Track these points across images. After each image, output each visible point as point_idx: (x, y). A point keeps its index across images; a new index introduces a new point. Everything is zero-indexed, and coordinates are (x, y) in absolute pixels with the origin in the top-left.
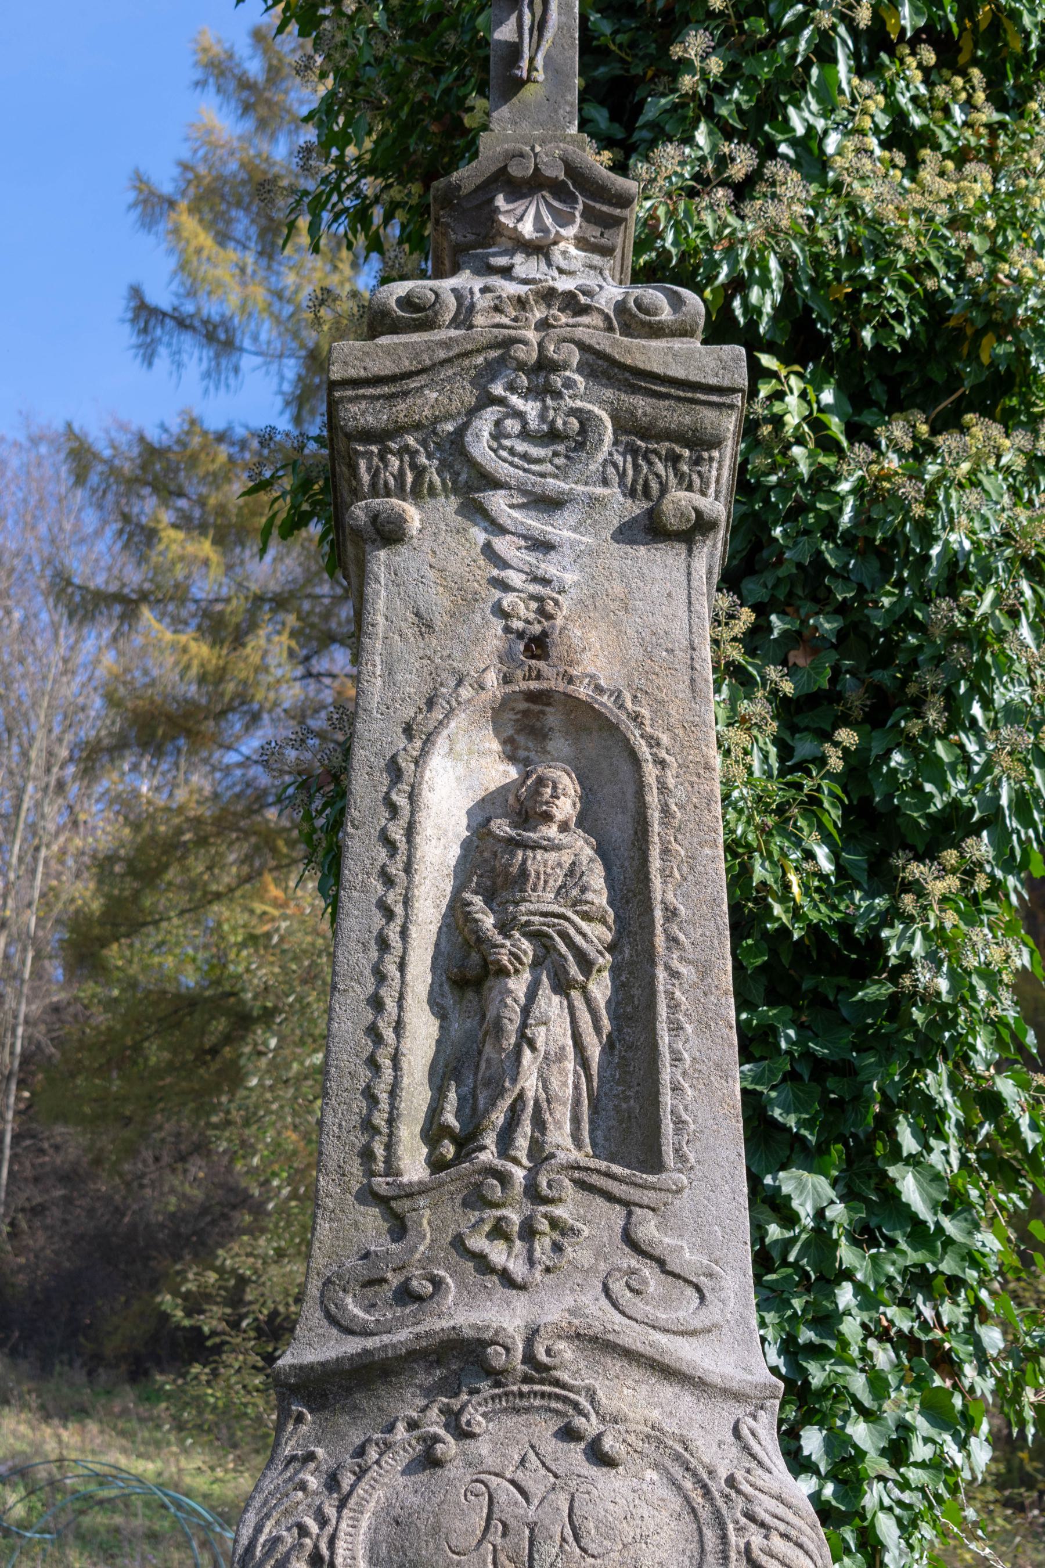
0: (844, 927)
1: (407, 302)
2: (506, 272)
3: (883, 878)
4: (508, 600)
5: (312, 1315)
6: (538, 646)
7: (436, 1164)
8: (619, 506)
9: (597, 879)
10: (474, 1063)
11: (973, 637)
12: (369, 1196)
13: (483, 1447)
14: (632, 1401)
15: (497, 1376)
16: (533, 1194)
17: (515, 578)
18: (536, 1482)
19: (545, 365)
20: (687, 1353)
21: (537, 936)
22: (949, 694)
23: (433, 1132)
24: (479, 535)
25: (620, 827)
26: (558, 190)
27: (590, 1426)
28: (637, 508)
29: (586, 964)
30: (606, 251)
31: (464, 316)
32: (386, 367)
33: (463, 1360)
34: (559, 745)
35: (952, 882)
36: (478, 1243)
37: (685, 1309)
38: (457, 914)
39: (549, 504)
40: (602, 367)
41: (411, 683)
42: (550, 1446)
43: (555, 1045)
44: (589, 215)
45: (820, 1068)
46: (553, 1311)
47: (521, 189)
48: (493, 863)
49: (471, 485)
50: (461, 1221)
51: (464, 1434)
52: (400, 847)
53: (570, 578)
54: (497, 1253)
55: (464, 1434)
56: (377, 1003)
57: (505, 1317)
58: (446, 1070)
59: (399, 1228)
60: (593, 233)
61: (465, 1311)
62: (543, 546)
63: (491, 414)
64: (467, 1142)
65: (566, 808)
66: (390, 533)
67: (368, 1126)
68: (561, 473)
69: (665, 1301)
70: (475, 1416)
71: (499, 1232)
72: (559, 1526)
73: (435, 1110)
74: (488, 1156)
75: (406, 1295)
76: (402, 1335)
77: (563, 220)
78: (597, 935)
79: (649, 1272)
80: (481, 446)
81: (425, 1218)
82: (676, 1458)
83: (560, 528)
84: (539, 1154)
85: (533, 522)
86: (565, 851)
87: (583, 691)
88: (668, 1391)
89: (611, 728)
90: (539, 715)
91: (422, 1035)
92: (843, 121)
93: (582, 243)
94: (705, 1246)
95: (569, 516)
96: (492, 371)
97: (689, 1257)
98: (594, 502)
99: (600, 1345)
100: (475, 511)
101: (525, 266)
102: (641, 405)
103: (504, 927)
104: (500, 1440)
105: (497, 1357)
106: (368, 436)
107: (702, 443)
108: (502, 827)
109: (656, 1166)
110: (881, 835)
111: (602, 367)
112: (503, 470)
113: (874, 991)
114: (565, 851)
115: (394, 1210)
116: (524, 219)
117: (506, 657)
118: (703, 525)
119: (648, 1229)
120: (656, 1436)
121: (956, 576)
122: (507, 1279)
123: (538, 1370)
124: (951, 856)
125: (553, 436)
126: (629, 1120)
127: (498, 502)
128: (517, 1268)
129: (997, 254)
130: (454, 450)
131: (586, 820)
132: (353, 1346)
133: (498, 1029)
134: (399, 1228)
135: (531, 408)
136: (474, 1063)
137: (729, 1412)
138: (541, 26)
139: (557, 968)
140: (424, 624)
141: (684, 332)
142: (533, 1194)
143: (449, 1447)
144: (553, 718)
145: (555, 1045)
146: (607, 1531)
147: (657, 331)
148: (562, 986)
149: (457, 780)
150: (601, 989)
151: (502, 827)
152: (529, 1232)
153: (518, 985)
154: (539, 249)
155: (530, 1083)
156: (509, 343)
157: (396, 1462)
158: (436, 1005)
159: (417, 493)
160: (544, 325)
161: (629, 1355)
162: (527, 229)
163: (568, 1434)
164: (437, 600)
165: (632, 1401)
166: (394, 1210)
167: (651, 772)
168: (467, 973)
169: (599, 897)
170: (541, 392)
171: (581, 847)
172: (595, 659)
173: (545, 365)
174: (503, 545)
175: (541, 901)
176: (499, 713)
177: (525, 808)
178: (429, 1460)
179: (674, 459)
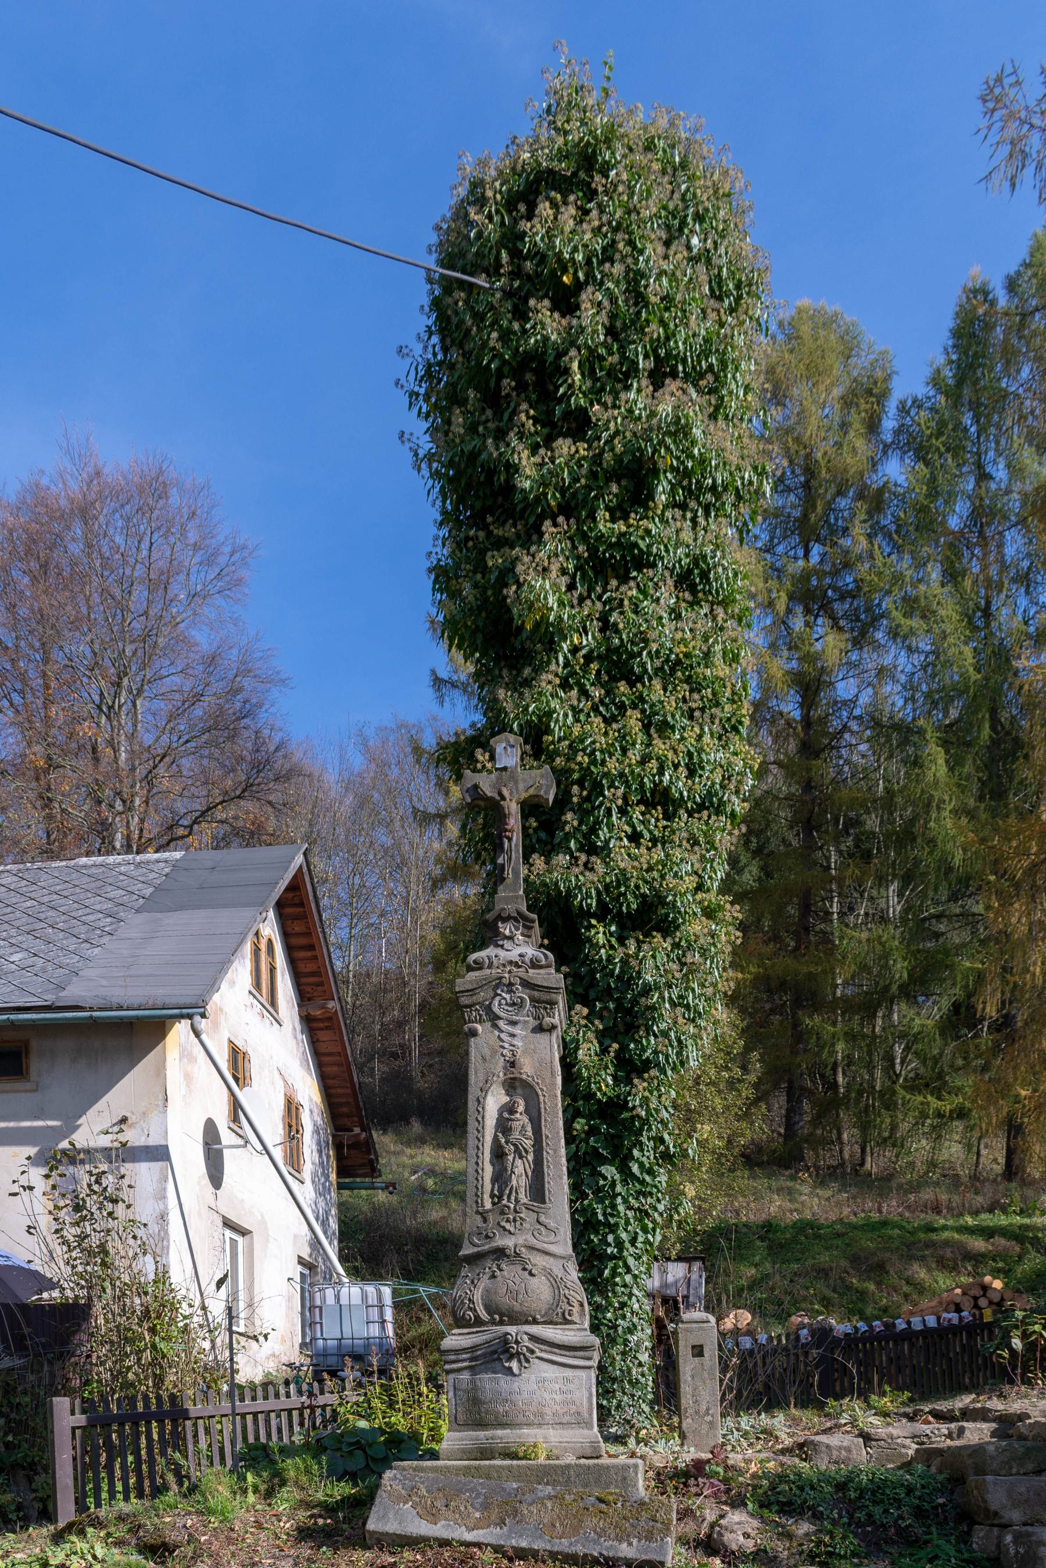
0: (618, 1096)
1: (475, 962)
2: (502, 946)
3: (629, 1082)
4: (505, 1052)
5: (466, 1242)
6: (513, 1064)
7: (494, 1204)
8: (532, 1023)
9: (529, 1128)
10: (501, 1178)
11: (653, 1008)
12: (478, 1212)
13: (505, 1273)
14: (539, 1261)
15: (508, 1256)
16: (515, 1211)
17: (506, 1045)
18: (517, 1280)
19: (511, 984)
20: (552, 1248)
21: (514, 1145)
22: (646, 1025)
23: (492, 1196)
24: (497, 1033)
25: (535, 1115)
26: (515, 919)
27: (529, 1267)
28: (537, 1023)
29: (527, 1152)
30: (529, 937)
31: (490, 966)
32: (469, 987)
33: (500, 1253)
34: (519, 1091)
35: (645, 1084)
36: (503, 1224)
37: (552, 1238)
38: (496, 1139)
39: (514, 1023)
40: (526, 984)
41: (481, 1077)
42: (521, 1272)
43: (520, 1171)
44: (524, 926)
45: (613, 1136)
46: (521, 1241)
47: (505, 920)
48: (504, 1126)
49: (494, 1018)
50: (499, 1218)
51: (501, 1270)
52: (481, 1122)
53: (520, 1044)
54: (508, 1226)
55: (501, 1270)
56: (477, 1164)
57: (509, 1242)
58: (495, 1180)
59: (485, 1220)
60: (526, 932)
61: (500, 1241)
62: (513, 1035)
63: (498, 998)
64: (500, 1198)
65: (521, 1108)
66: (474, 1033)
67: (477, 1195)
68: (517, 1014)
69: (547, 1236)
70: (503, 1266)
71: (508, 1221)
72: (523, 1291)
73: (492, 1190)
74: (504, 1202)
75: (487, 1237)
76: (486, 1247)
77: (517, 929)
78: (528, 1143)
79: (543, 1229)
80: (496, 1008)
81: (491, 1217)
82: (549, 1274)
83: (517, 1030)
84: (517, 1201)
85: (510, 1029)
86: (521, 1120)
87: (524, 1077)
88: (547, 1258)
89: (531, 1087)
90: (512, 1085)
91: (488, 1171)
92: (613, 834)
93: (523, 935)
94: (556, 1222)
95: (519, 1026)
96: (497, 986)
97: (552, 1224)
98: (525, 1022)
99: (531, 1248)
100: (495, 1026)
101: (507, 944)
102: (536, 994)
103: (507, 1142)
104: (509, 1272)
105: (508, 1252)
106: (467, 1006)
107: (553, 1003)
108: (506, 1115)
109: (544, 1202)
110: (630, 1068)
111: (526, 984)
112: (502, 1014)
113: (625, 1115)
114: (521, 1120)
115: (484, 1216)
116: (506, 929)
117: (505, 1068)
118: (554, 1027)
119: (543, 1219)
120: (544, 1269)
121: (647, 990)
122: (510, 1233)
123: (517, 1255)
124: (646, 1075)
125: (514, 1004)
126: (538, 1191)
127: (501, 1024)
128: (512, 1229)
129: (663, 877)
130: (489, 1009)
131: (527, 1111)
132: (476, 1250)
133: (506, 1170)
134: (485, 1220)
135: (507, 996)
136: (501, 1178)
137: (561, 1262)
138: (510, 859)
139: (519, 1153)
140: (484, 1059)
141: (548, 966)
142: (515, 1211)
143: (498, 1273)
144: (517, 1084)
145: (520, 1171)
146: (533, 1291)
147: (541, 967)
148: (521, 1157)
149: (494, 1101)
150: (531, 1157)
151: (506, 1115)
152: (515, 1220)
153: (511, 1158)
154: (511, 938)
155: (514, 1183)
156: (501, 978)
157: (486, 1277)
158: (492, 1163)
159: (480, 1022)
160: (510, 972)
161: (538, 1250)
162: (507, 932)
163: (524, 1269)
164: (487, 1052)
165: (539, 1261)
166: (484, 1216)
167: (541, 1098)
168: (499, 1154)
169: (530, 1133)
170: (510, 992)
171: (525, 1119)
172: (527, 1068)
173: (511, 984)
174: (502, 1036)
175: (516, 1135)
176: (503, 1084)
177: (509, 1109)
178: (493, 1276)
179: (545, 1008)
